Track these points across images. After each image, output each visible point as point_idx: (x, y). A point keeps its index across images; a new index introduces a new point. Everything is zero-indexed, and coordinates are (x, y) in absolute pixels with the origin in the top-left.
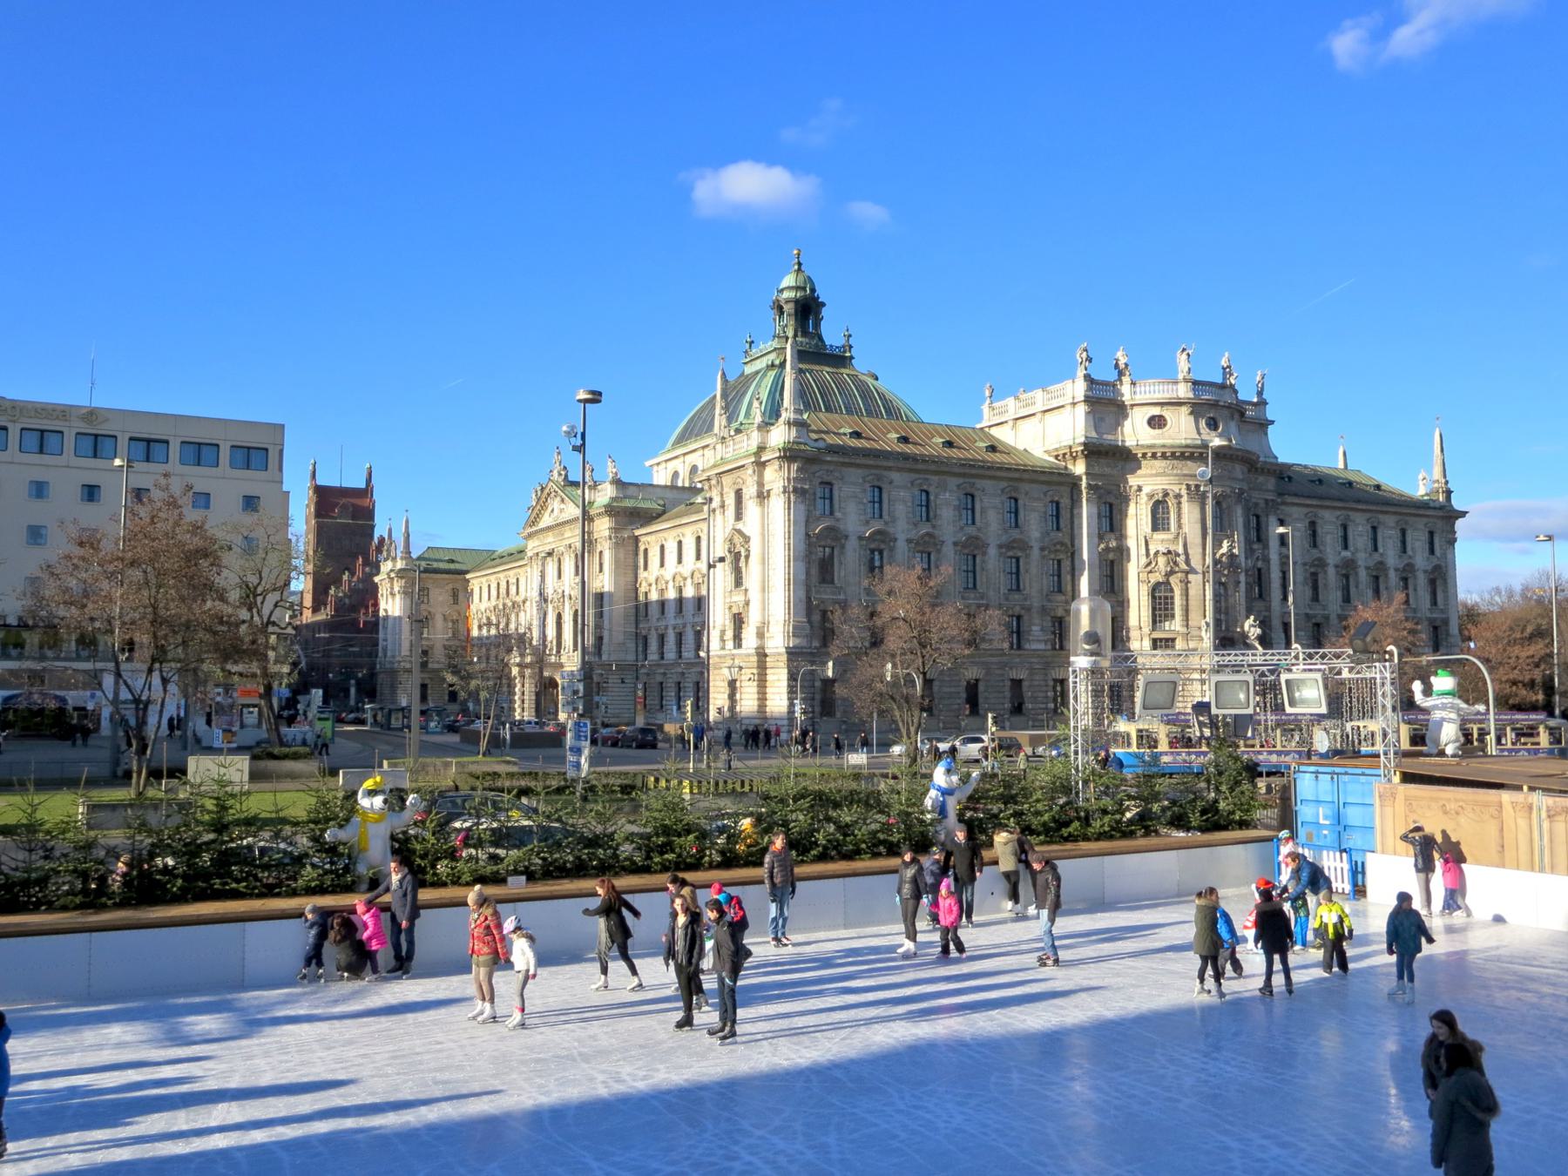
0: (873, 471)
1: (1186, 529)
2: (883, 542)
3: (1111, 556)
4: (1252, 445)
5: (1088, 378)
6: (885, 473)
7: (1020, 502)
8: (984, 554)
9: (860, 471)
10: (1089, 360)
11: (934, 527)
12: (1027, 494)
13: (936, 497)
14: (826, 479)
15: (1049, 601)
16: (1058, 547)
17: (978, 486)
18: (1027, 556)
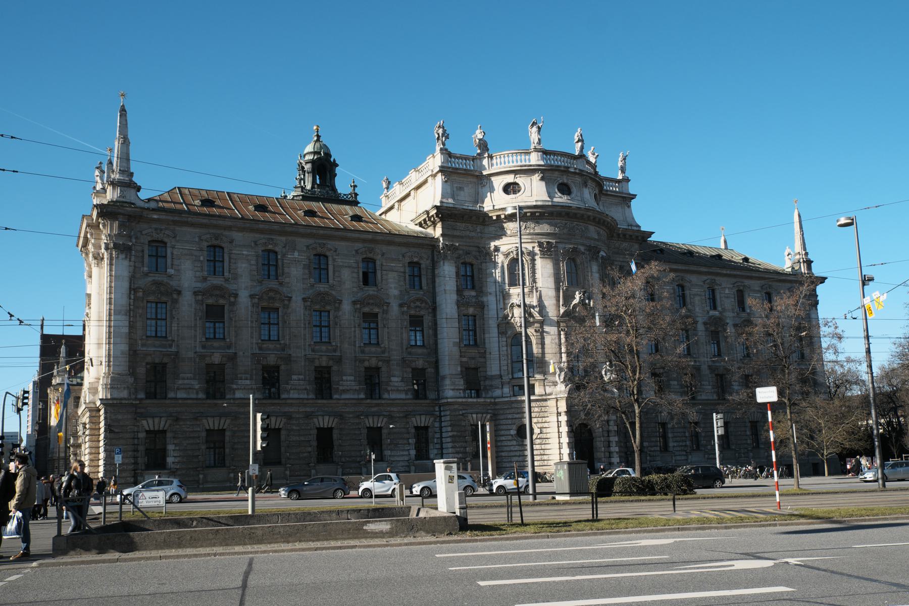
0: (212, 231)
1: (540, 284)
2: (223, 297)
3: (471, 311)
4: (615, 213)
5: (444, 151)
6: (226, 233)
7: (378, 263)
8: (338, 309)
9: (197, 230)
10: (446, 135)
11: (281, 284)
12: (383, 255)
13: (284, 255)
14: (156, 236)
15: (410, 353)
16: (418, 303)
17: (329, 246)
18: (386, 312)
